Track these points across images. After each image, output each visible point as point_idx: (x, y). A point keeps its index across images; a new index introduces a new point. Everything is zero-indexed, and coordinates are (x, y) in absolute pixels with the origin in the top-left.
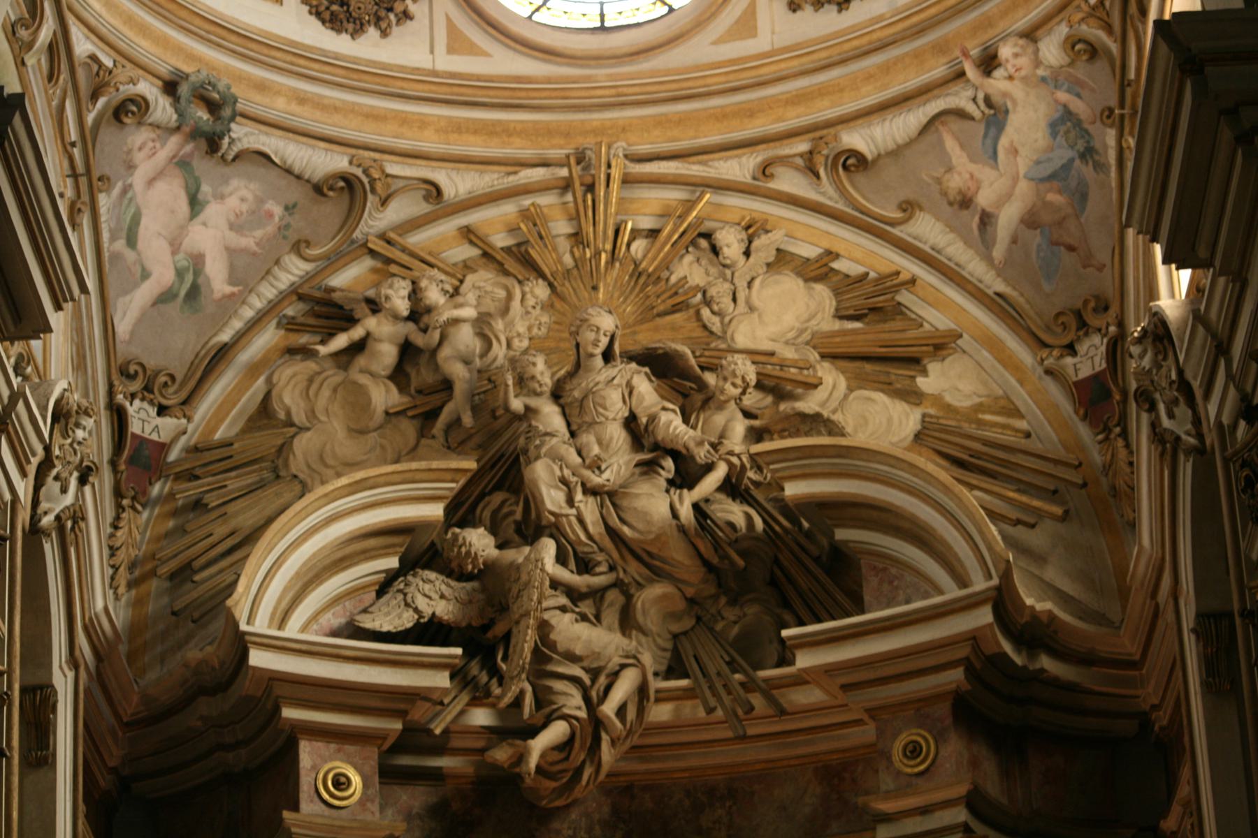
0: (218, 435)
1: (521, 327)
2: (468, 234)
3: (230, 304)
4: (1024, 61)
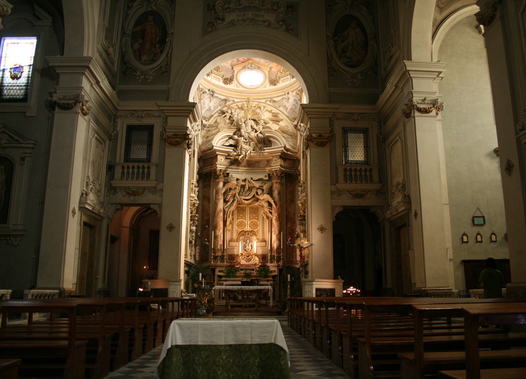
0: (211, 124)
1: (241, 115)
2: (237, 105)
3: (213, 111)
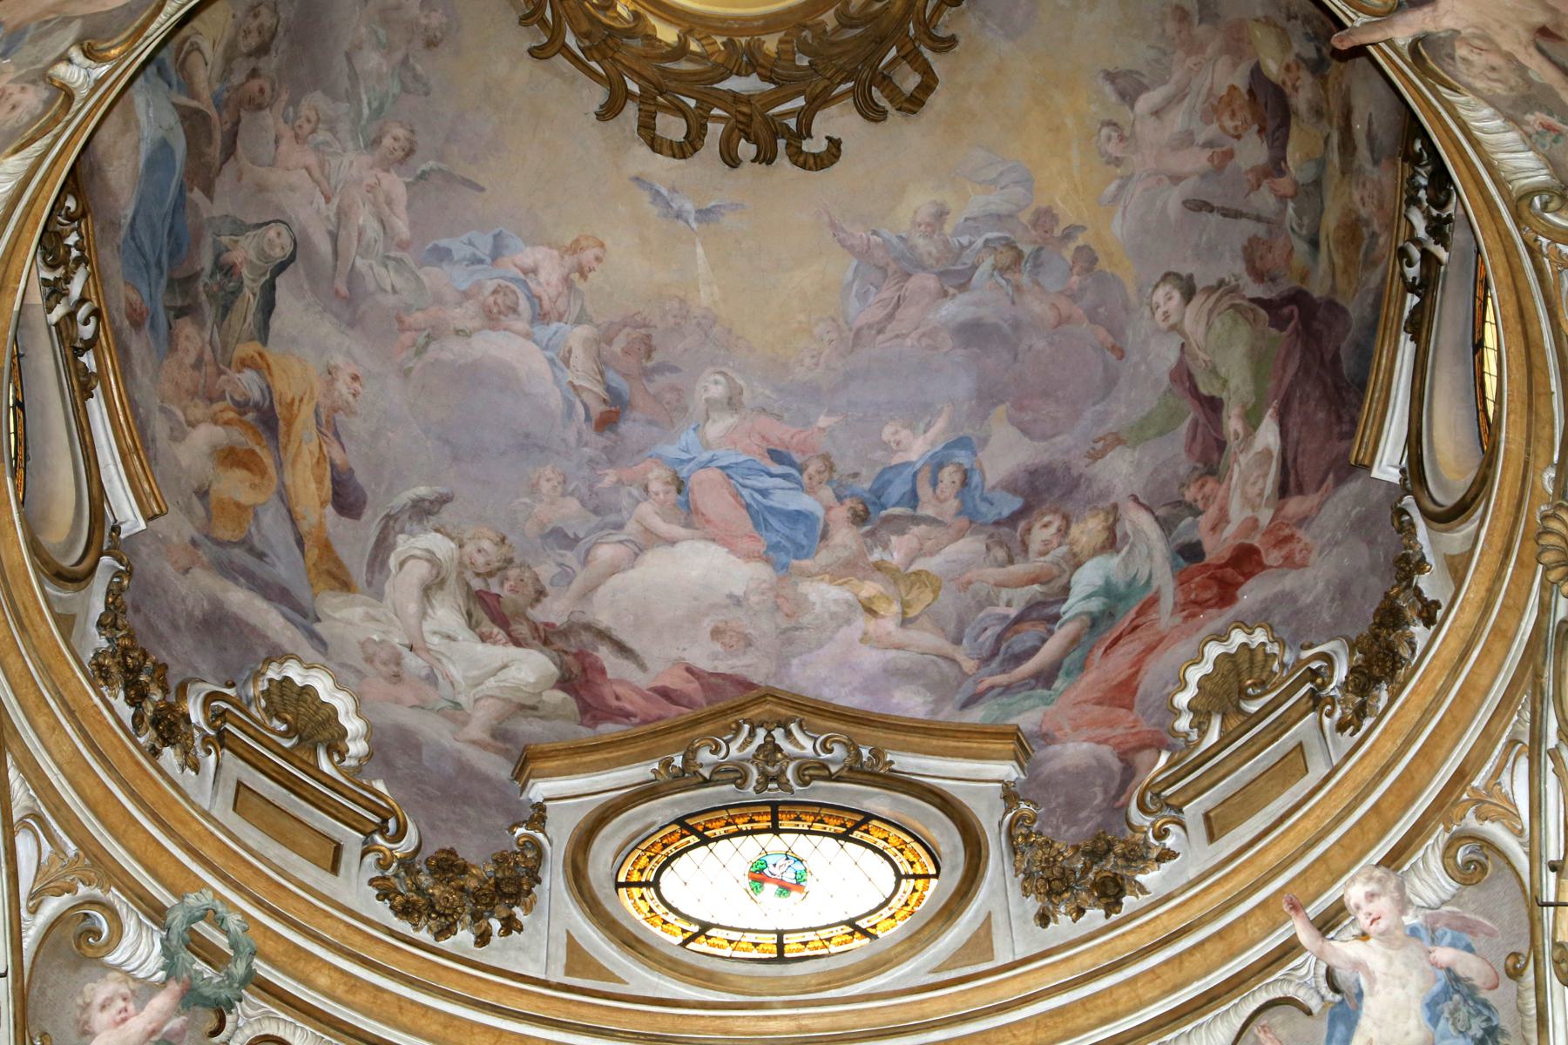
4: (1383, 905)
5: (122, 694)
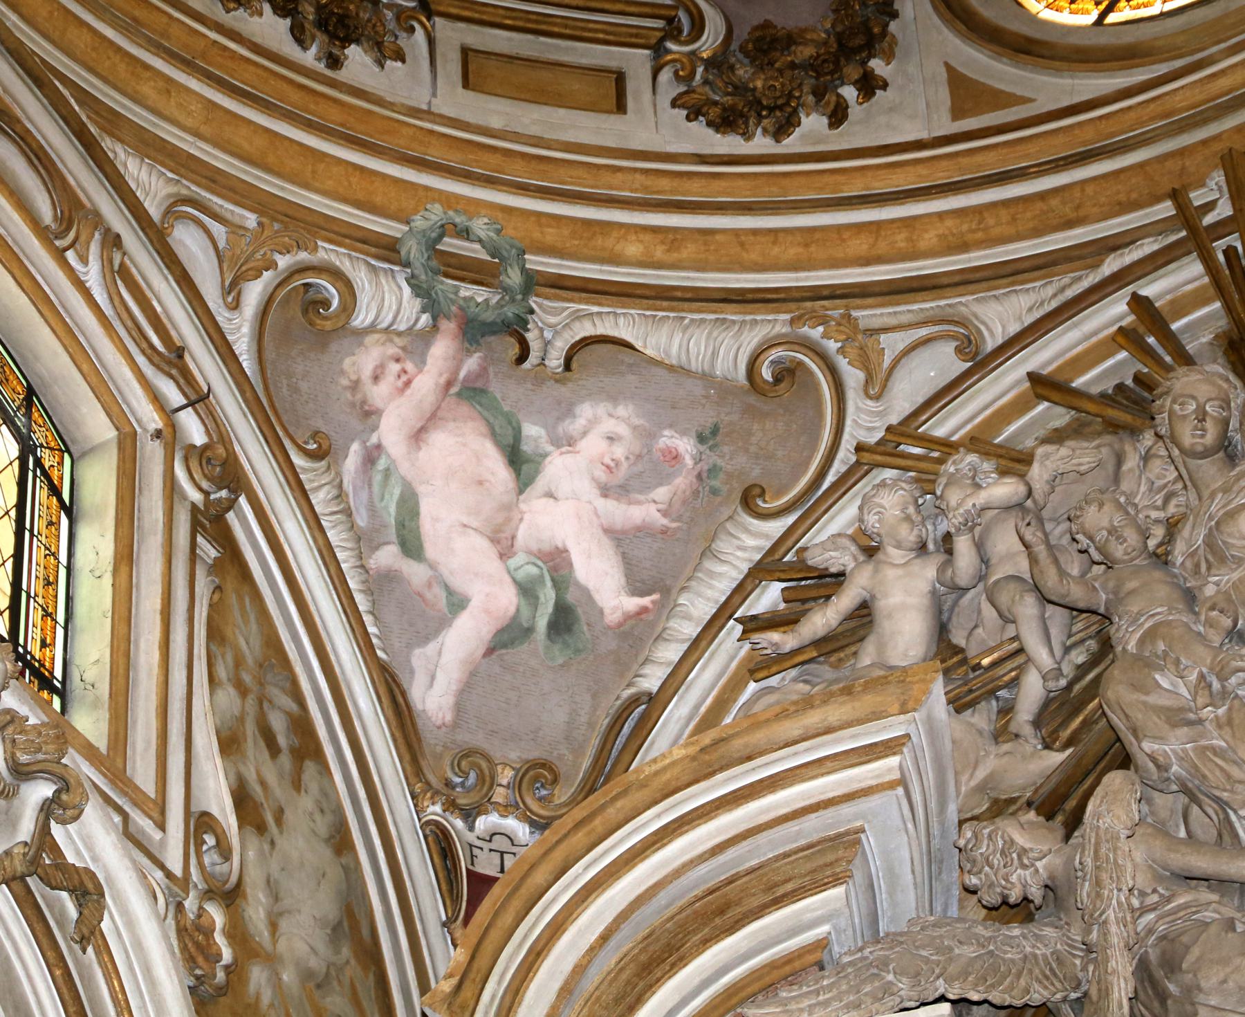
5: (267, 8)
